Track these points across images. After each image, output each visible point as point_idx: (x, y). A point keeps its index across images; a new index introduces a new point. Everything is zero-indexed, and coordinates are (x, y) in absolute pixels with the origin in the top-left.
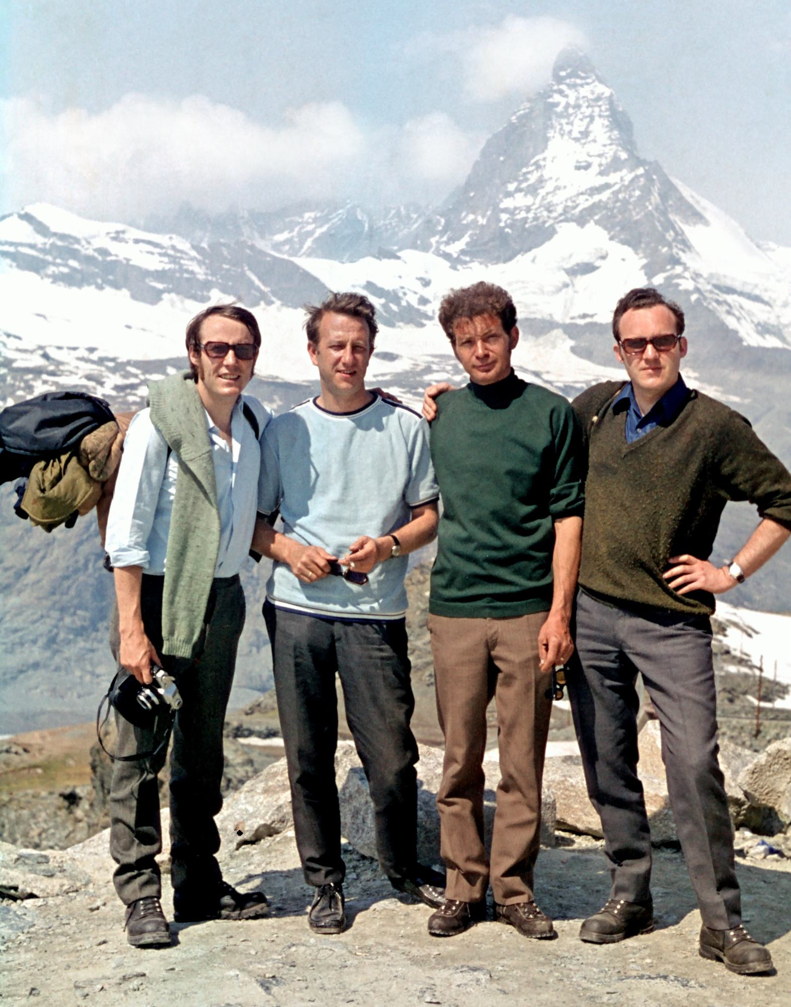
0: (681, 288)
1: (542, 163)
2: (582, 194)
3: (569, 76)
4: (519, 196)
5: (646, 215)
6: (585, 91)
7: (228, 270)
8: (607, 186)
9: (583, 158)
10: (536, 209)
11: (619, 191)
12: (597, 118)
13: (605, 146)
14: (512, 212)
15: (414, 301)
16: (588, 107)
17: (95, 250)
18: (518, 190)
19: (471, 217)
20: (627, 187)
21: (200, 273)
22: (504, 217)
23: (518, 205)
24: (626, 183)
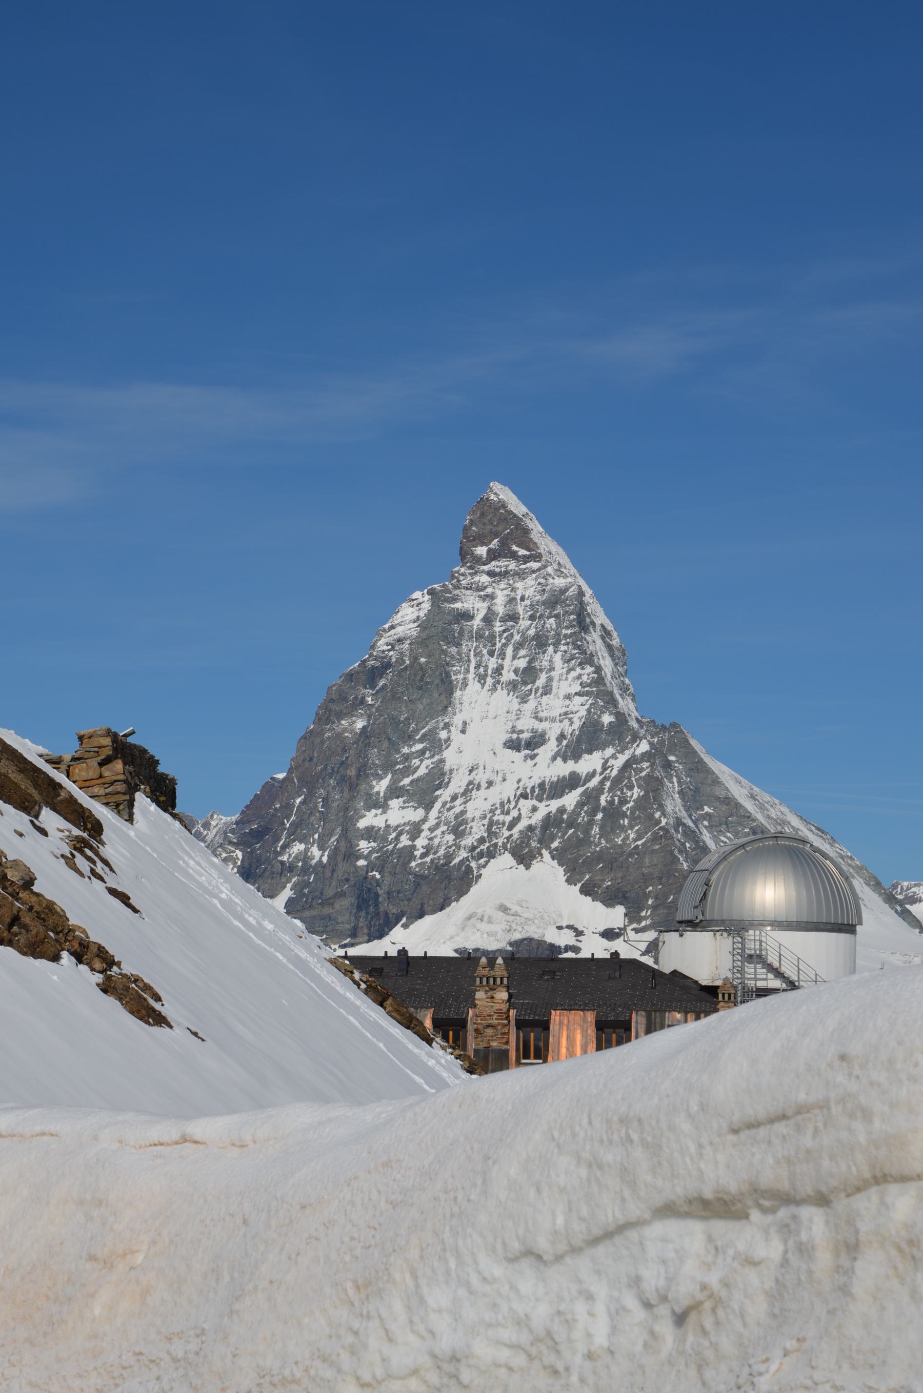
1: (443, 735)
2: (524, 796)
3: (493, 555)
4: (394, 803)
5: (655, 838)
6: (528, 588)
8: (572, 781)
9: (527, 724)
10: (432, 830)
11: (599, 790)
13: (568, 697)
16: (532, 618)
18: (395, 791)
19: (298, 847)
20: (617, 781)
22: (364, 846)
23: (393, 822)
24: (615, 773)
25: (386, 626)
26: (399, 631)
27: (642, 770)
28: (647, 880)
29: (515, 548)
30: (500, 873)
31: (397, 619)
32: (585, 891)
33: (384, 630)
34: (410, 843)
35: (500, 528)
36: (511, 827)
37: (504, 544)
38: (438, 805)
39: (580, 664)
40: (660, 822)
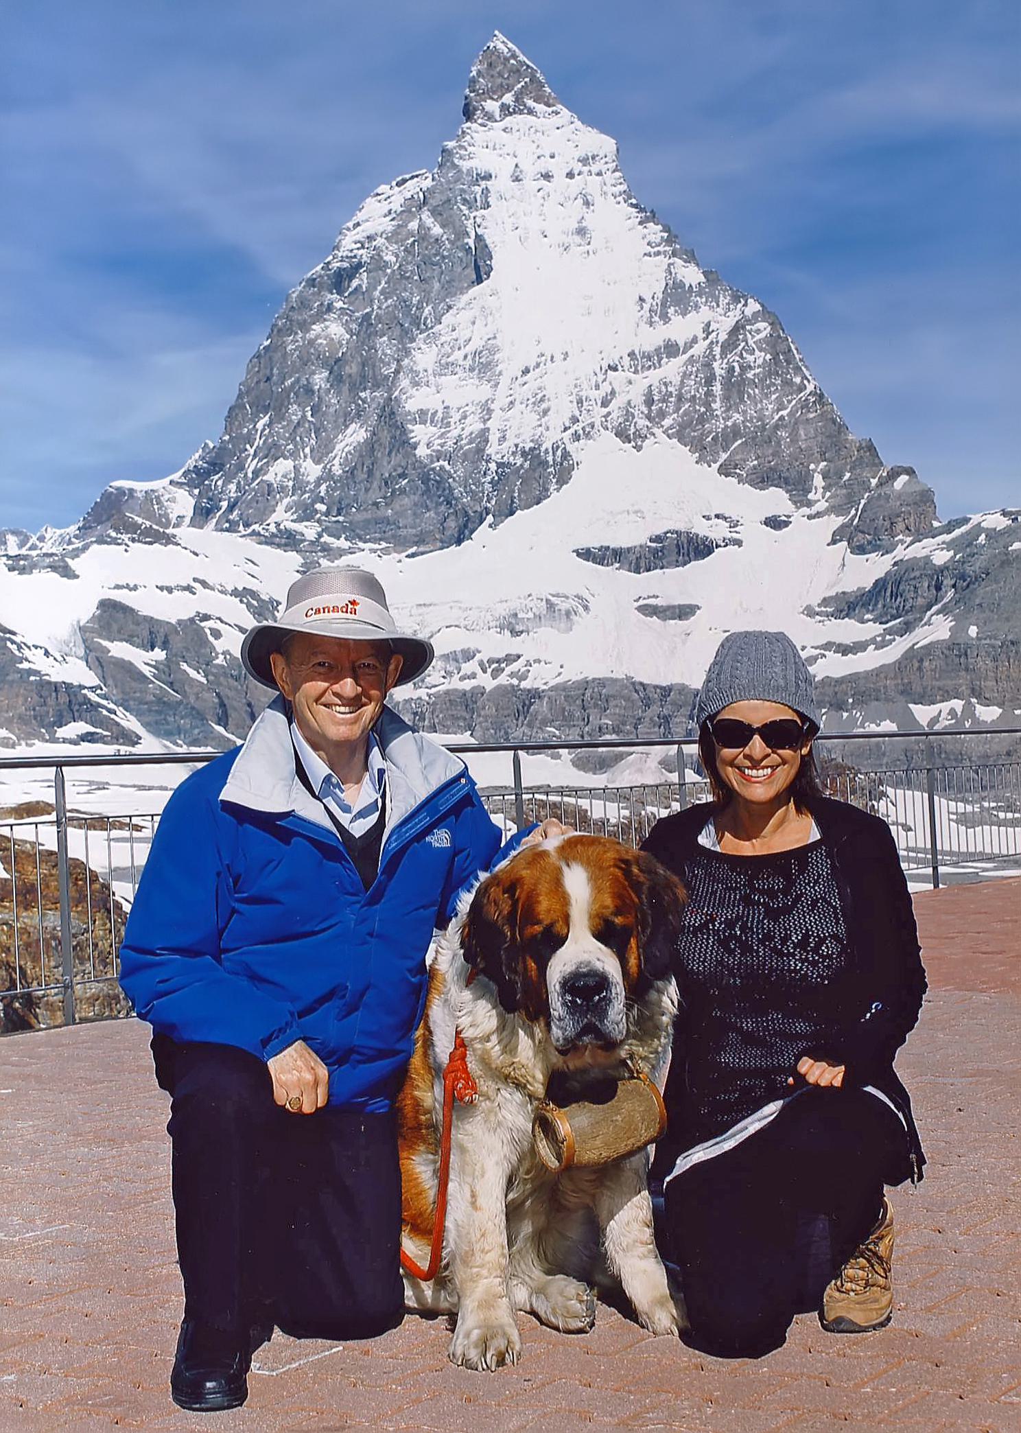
4: (447, 380)
8: (671, 349)
12: (598, 200)
16: (570, 175)
18: (446, 367)
20: (729, 346)
24: (723, 337)
25: (350, 224)
26: (367, 229)
27: (758, 331)
31: (360, 216)
33: (348, 229)
34: (482, 426)
35: (511, 81)
36: (605, 404)
37: (518, 99)
38: (504, 381)
39: (640, 223)
40: (802, 388)
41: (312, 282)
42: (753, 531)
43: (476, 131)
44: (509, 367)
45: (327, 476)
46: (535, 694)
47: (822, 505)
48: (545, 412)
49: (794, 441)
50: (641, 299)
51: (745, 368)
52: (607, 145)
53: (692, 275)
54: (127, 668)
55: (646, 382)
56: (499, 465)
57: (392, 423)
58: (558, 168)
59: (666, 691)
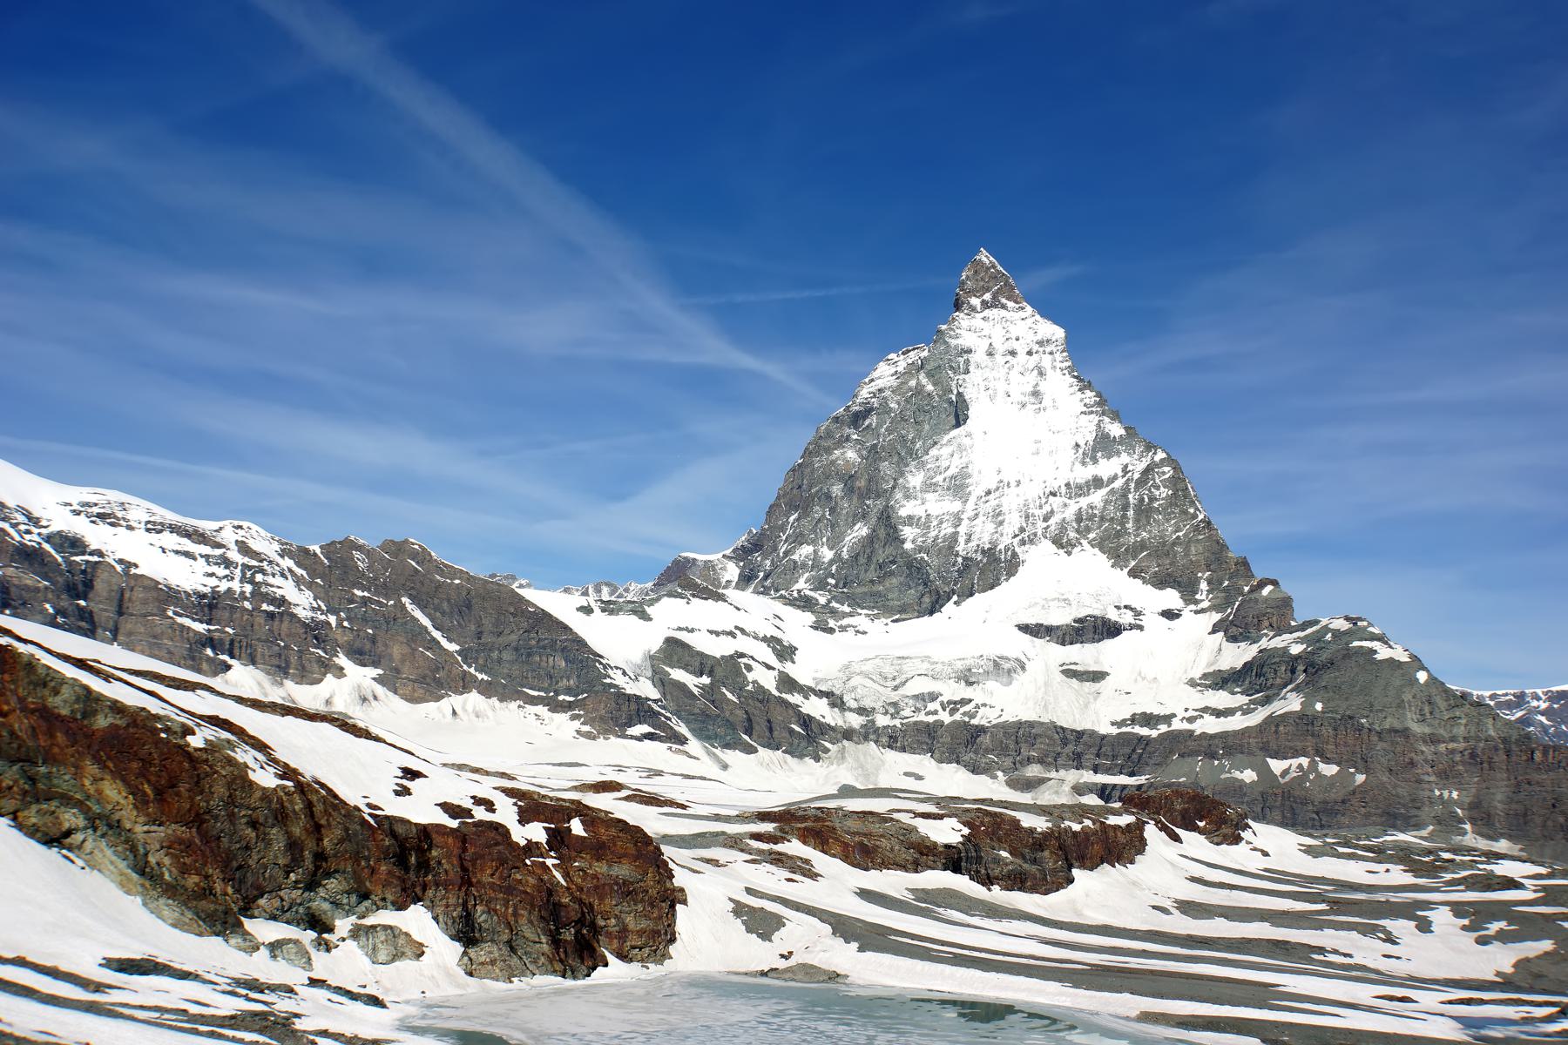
0: (1379, 657)
1: (967, 441)
2: (1054, 494)
4: (930, 496)
7: (365, 601)
8: (1097, 482)
11: (1125, 492)
12: (1049, 372)
14: (924, 523)
15: (768, 681)
16: (1030, 353)
17: (49, 539)
18: (930, 486)
19: (807, 550)
20: (1141, 483)
21: (303, 603)
24: (1137, 476)
26: (880, 384)
28: (1193, 567)
29: (1004, 301)
30: (1040, 559)
31: (875, 374)
32: (1134, 574)
36: (1046, 519)
37: (994, 297)
38: (972, 499)
40: (1195, 516)
41: (836, 419)
42: (1152, 621)
43: (962, 319)
44: (976, 491)
45: (838, 558)
46: (981, 730)
47: (1206, 604)
48: (1001, 523)
49: (1187, 553)
50: (1077, 445)
51: (1152, 499)
52: (1058, 333)
53: (1116, 430)
54: (682, 687)
55: (1077, 507)
56: (965, 559)
57: (888, 525)
58: (1021, 348)
59: (1079, 734)
